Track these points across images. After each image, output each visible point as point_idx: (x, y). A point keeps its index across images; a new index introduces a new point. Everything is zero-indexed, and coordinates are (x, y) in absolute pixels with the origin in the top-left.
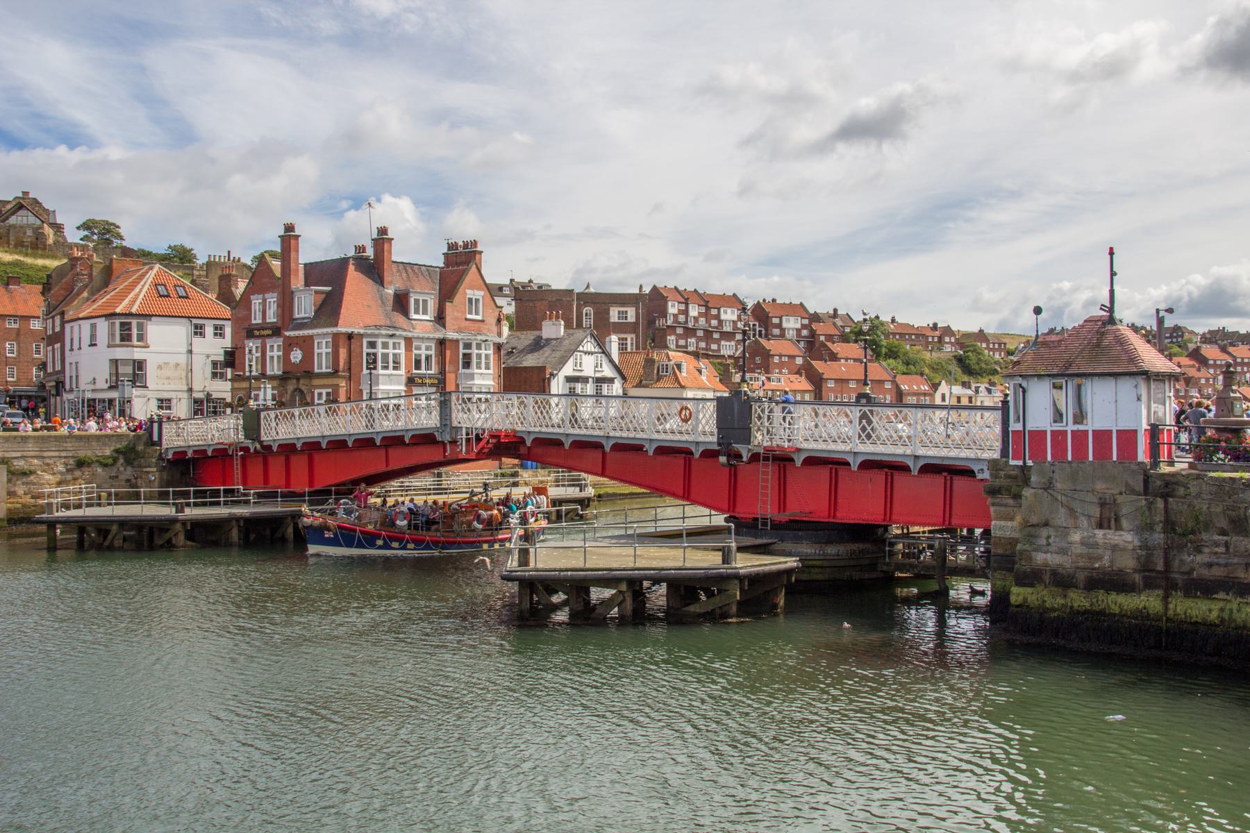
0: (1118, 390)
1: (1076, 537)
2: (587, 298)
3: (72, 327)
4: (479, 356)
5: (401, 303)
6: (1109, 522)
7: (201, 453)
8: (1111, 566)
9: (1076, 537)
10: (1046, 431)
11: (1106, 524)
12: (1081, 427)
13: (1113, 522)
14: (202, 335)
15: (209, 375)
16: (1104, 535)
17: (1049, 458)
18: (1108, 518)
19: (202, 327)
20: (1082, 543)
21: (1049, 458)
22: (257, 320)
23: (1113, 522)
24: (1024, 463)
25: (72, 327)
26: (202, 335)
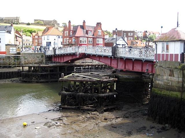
0: (175, 45)
1: (165, 78)
2: (124, 32)
3: (44, 37)
4: (100, 41)
5: (87, 33)
6: (172, 75)
7: (61, 55)
8: (171, 85)
9: (165, 78)
10: (178, 54)
11: (171, 76)
12: (167, 53)
13: (172, 75)
14: (60, 38)
15: (61, 44)
16: (171, 78)
17: (161, 60)
18: (172, 74)
19: (60, 37)
20: (166, 79)
21: (161, 60)
22: (65, 36)
23: (172, 75)
24: (156, 61)
25: (44, 37)
26: (60, 38)
